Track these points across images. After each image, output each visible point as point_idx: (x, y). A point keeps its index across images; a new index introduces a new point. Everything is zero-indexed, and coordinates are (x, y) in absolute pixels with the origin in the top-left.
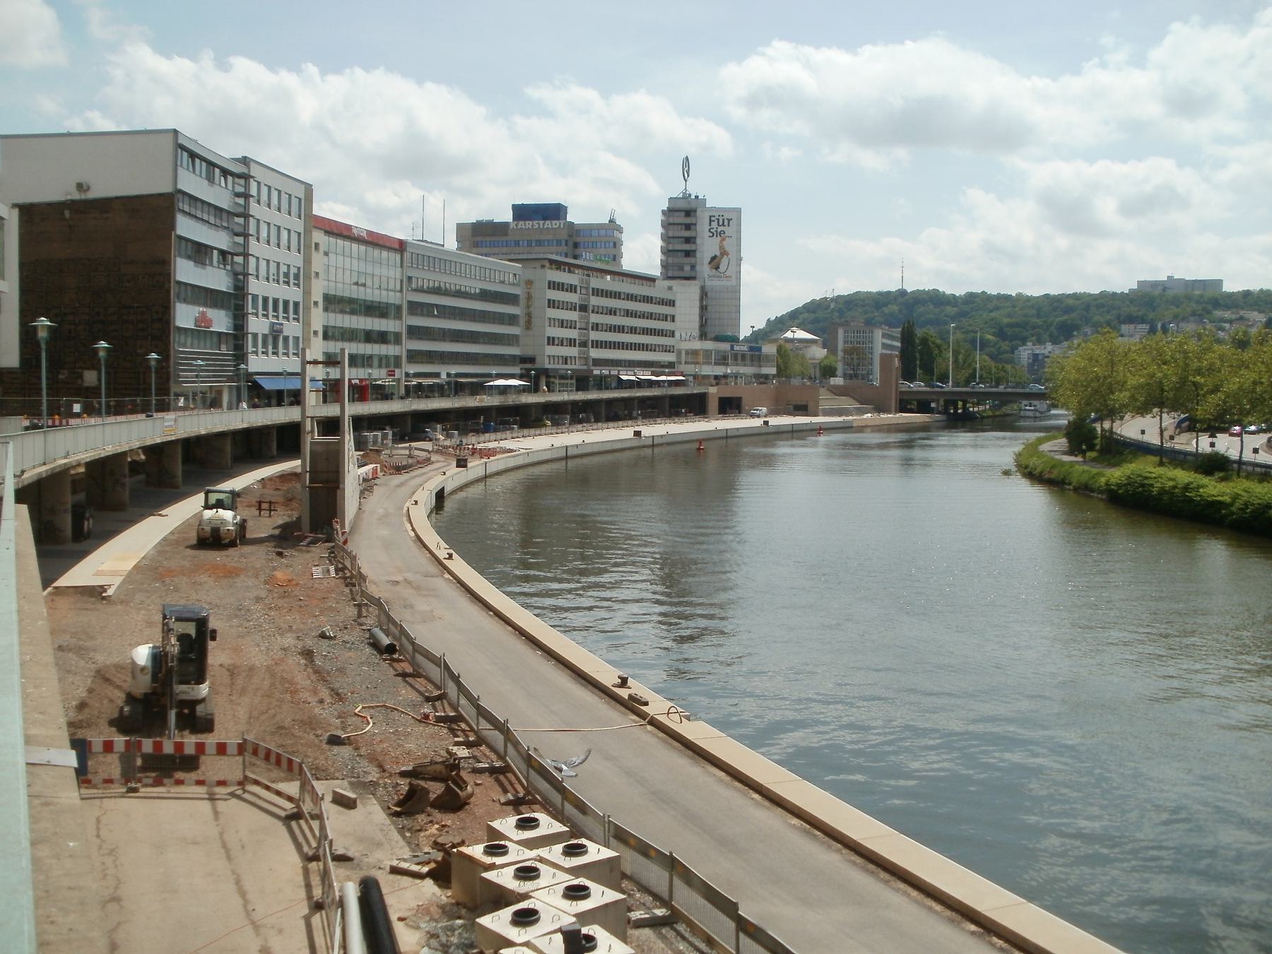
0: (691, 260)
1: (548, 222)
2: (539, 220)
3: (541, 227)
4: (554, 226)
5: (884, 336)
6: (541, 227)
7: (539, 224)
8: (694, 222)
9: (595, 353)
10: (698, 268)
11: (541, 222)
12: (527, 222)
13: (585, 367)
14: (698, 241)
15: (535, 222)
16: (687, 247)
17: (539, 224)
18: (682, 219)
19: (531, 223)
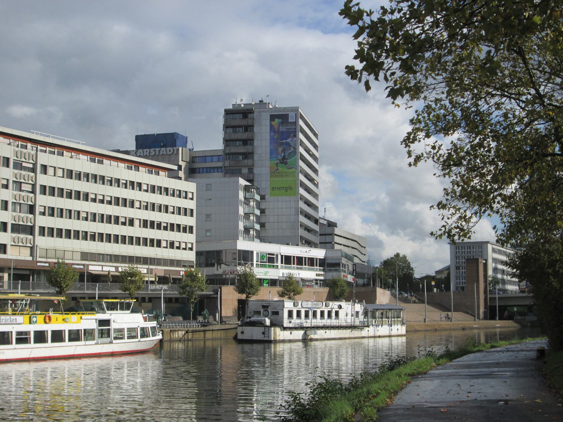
0: (248, 162)
1: (163, 149)
2: (155, 148)
3: (157, 154)
4: (168, 153)
5: (494, 250)
6: (157, 154)
7: (155, 151)
8: (250, 123)
9: (43, 242)
10: (256, 171)
11: (157, 150)
12: (145, 150)
13: (31, 259)
14: (256, 143)
15: (152, 150)
16: (242, 149)
17: (155, 151)
18: (238, 120)
19: (148, 150)
